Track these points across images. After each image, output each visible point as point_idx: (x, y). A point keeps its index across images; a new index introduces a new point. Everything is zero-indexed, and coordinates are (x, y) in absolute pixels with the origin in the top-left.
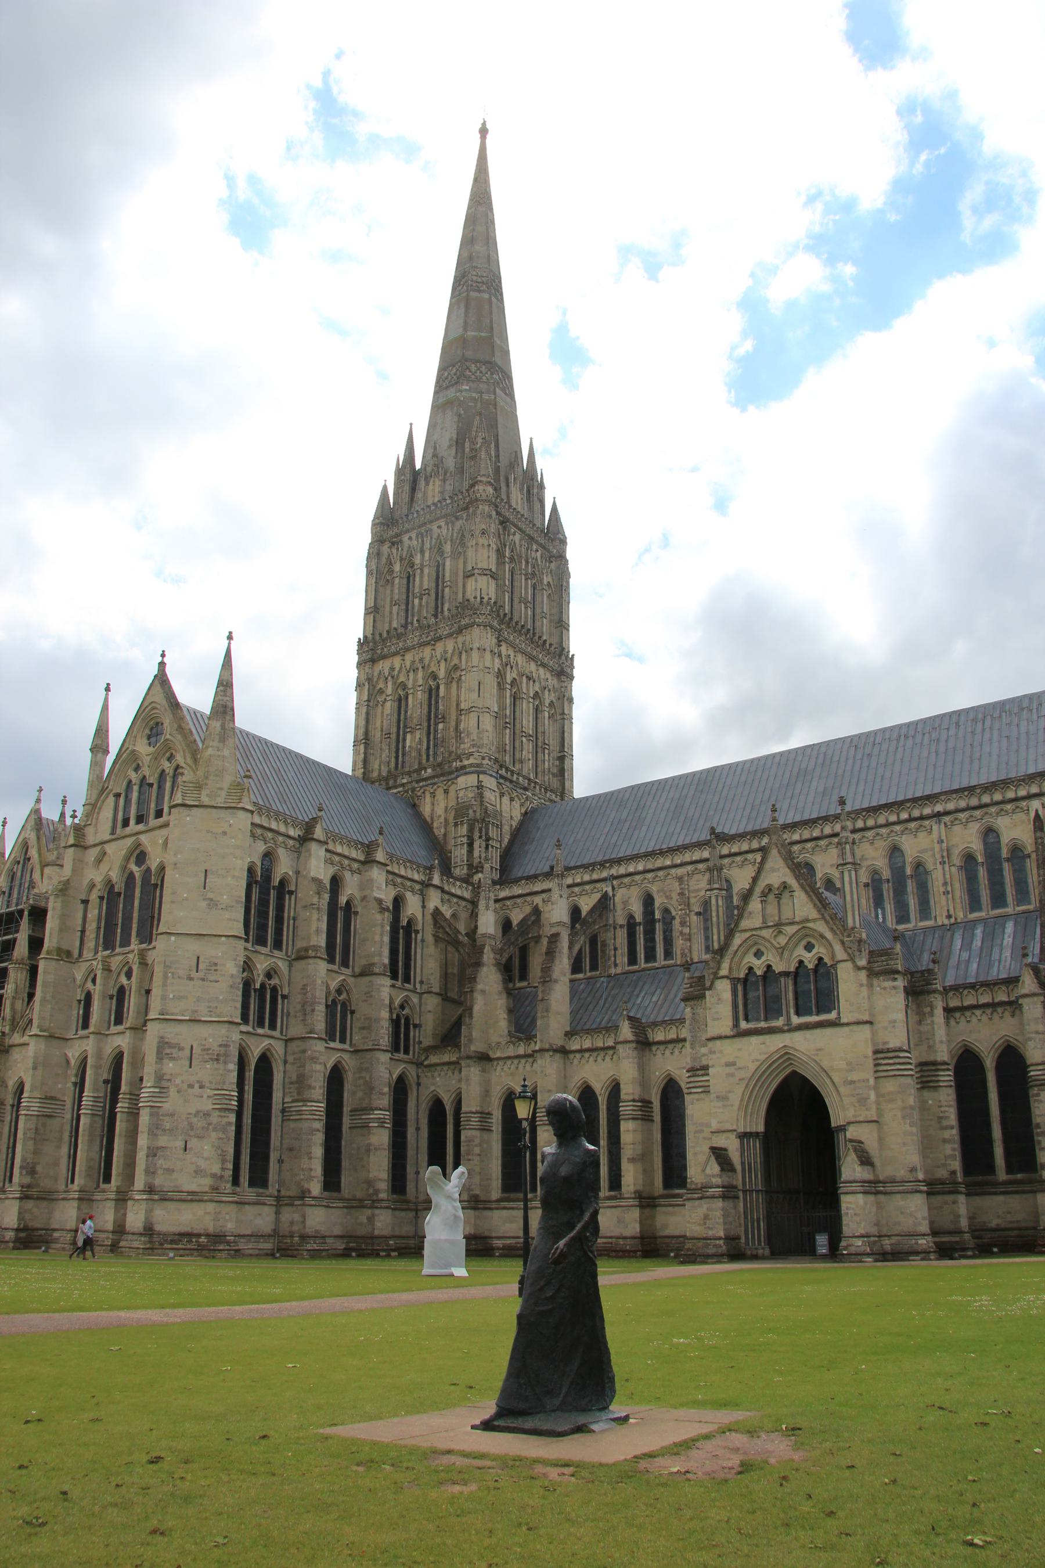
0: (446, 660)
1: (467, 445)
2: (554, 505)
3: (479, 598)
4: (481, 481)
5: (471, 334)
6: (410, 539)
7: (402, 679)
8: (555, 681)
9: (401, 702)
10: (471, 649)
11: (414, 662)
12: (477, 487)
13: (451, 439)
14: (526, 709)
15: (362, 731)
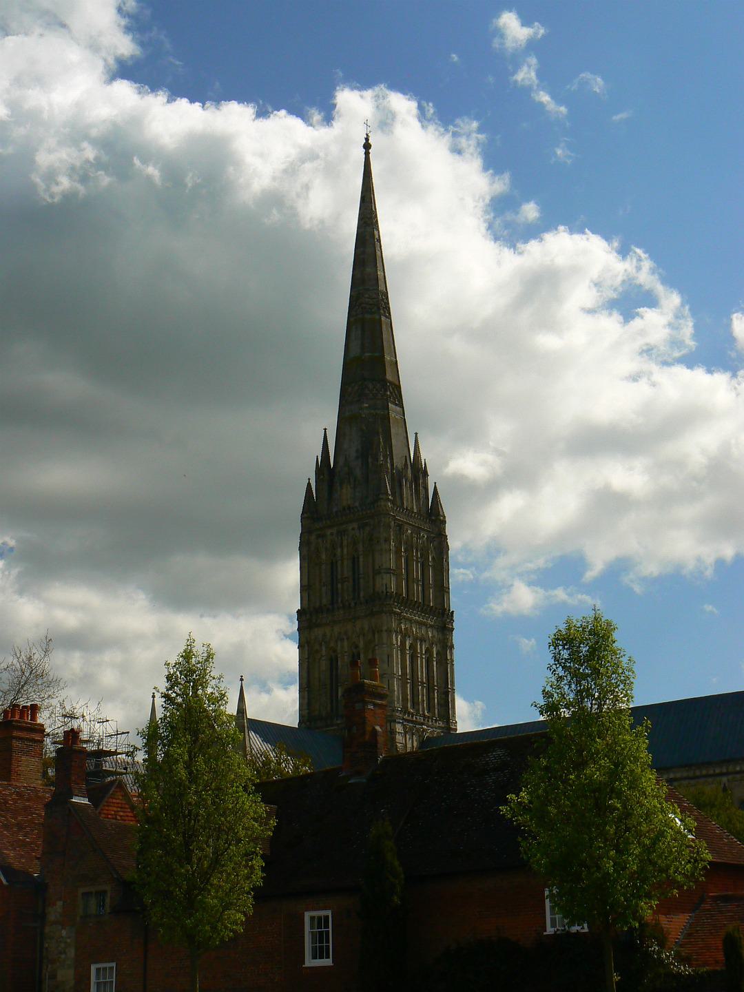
0: (364, 635)
1: (370, 460)
2: (435, 487)
3: (385, 592)
4: (382, 499)
5: (367, 354)
6: (332, 534)
7: (332, 644)
8: (440, 636)
9: (333, 662)
10: (382, 631)
11: (340, 633)
12: (379, 503)
13: (357, 451)
14: (421, 663)
15: (305, 681)
